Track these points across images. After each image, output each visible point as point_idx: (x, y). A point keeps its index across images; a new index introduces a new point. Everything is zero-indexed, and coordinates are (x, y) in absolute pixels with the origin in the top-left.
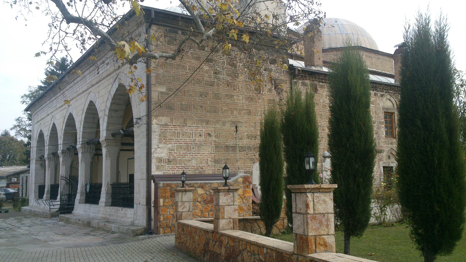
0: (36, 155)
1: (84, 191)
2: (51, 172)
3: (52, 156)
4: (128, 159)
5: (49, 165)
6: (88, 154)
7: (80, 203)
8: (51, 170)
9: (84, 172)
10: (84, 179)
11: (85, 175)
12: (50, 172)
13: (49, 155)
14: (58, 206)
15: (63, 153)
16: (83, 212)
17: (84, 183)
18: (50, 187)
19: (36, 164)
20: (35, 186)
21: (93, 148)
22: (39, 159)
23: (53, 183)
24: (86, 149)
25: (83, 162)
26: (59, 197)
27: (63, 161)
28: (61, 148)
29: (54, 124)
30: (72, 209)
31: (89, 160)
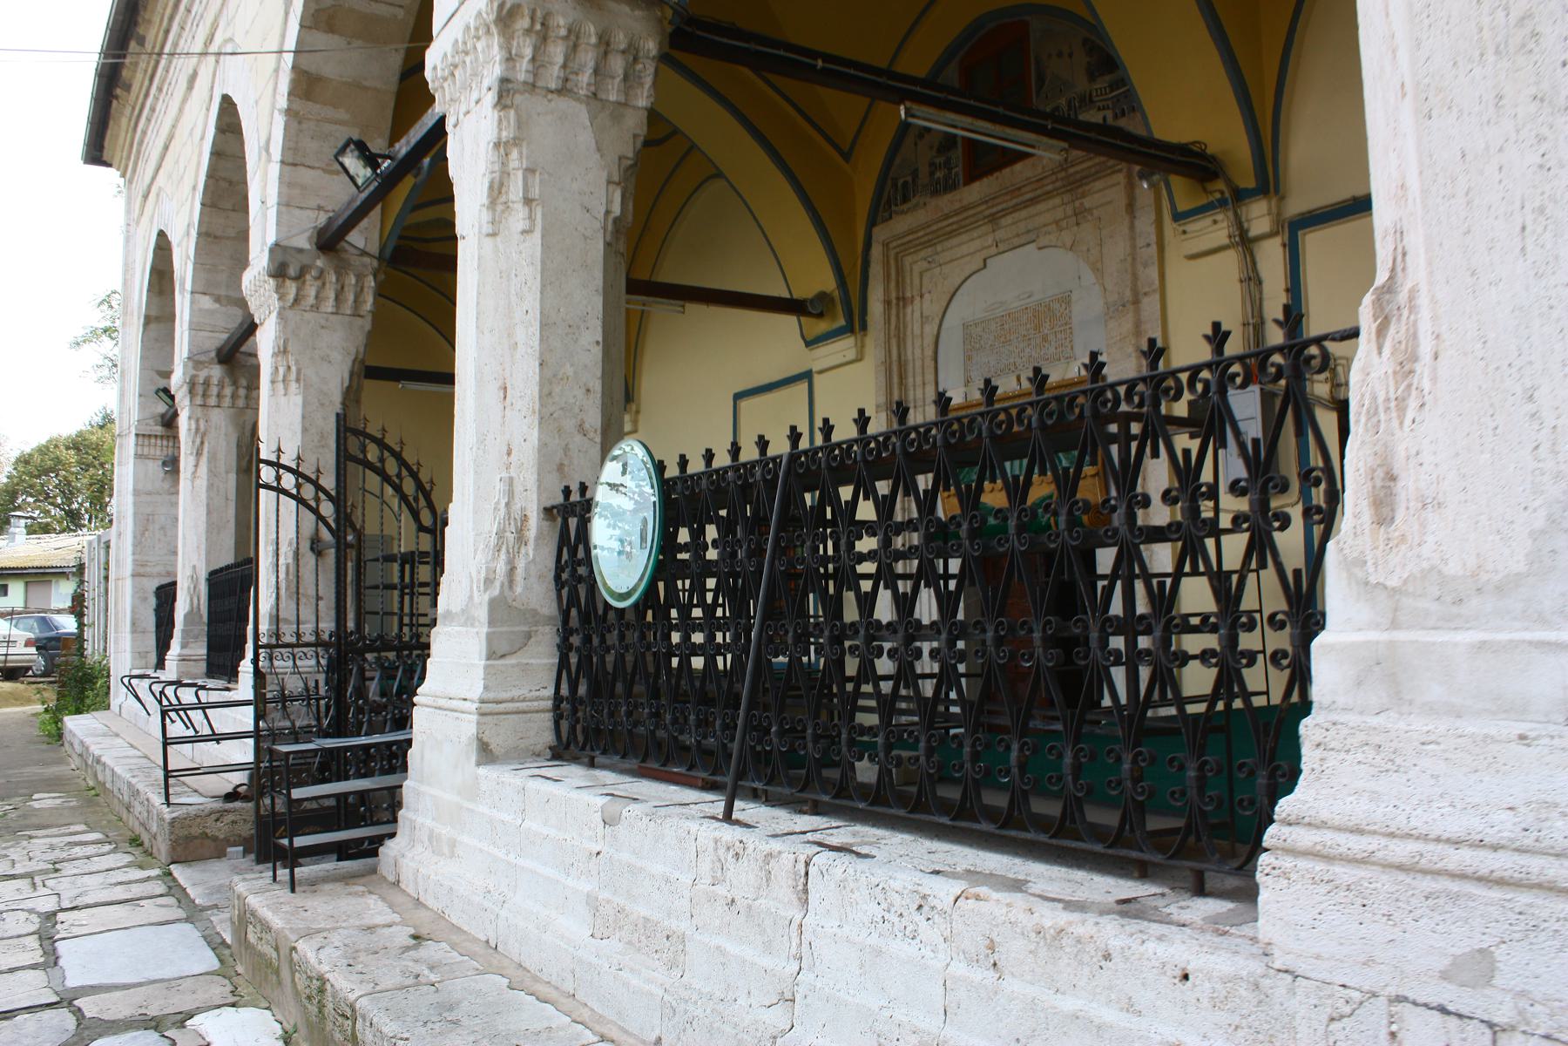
0: (142, 407)
1: (539, 596)
2: (210, 487)
3: (216, 372)
4: (738, 397)
5: (201, 435)
6: (581, 113)
7: (486, 753)
8: (212, 473)
9: (528, 336)
10: (525, 433)
11: (546, 395)
12: (202, 483)
13: (195, 360)
14: (243, 752)
15: (279, 272)
16: (574, 926)
17: (527, 479)
18: (203, 588)
19: (138, 456)
20: (138, 593)
21: (633, 53)
22: (159, 430)
23: (227, 558)
24: (557, 52)
25: (518, 219)
26: (246, 667)
27: (282, 351)
28: (264, 227)
29: (227, 101)
30: (382, 811)
31: (592, 194)
